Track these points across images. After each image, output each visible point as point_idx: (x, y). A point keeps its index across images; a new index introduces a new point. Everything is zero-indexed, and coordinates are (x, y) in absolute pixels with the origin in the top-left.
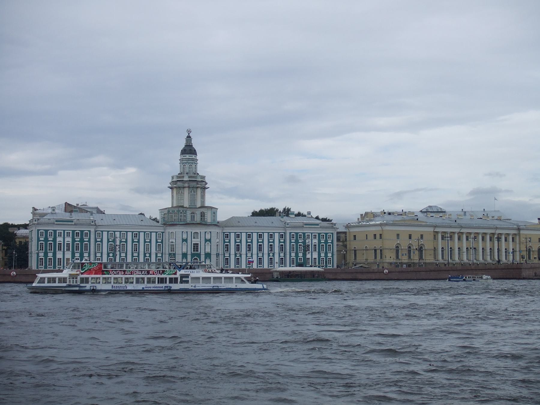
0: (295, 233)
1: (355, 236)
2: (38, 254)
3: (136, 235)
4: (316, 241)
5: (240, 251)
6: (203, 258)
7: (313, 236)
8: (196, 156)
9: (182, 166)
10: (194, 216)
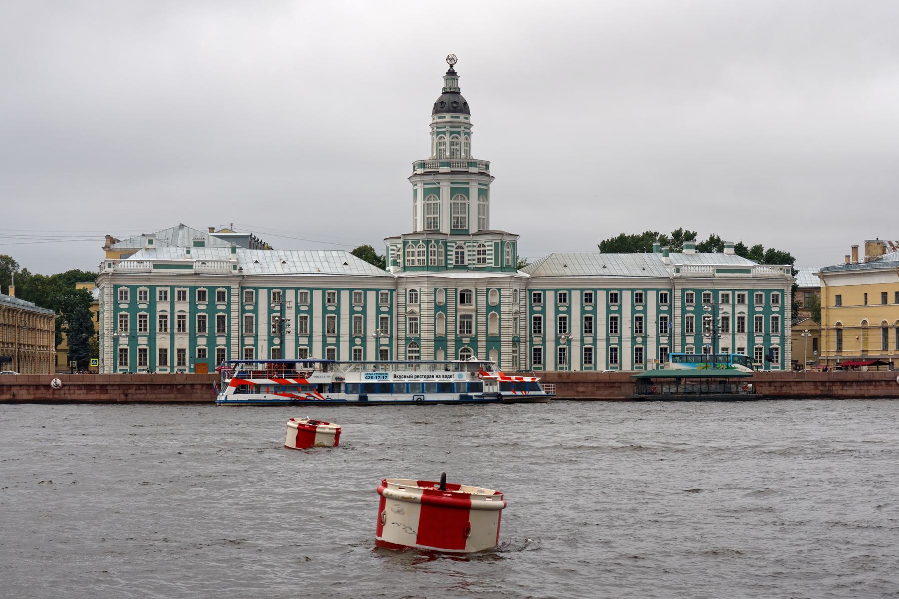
0: (694, 290)
1: (839, 298)
2: (116, 340)
3: (331, 297)
4: (742, 309)
5: (567, 332)
6: (482, 346)
8: (466, 116)
9: (436, 140)
10: (463, 253)
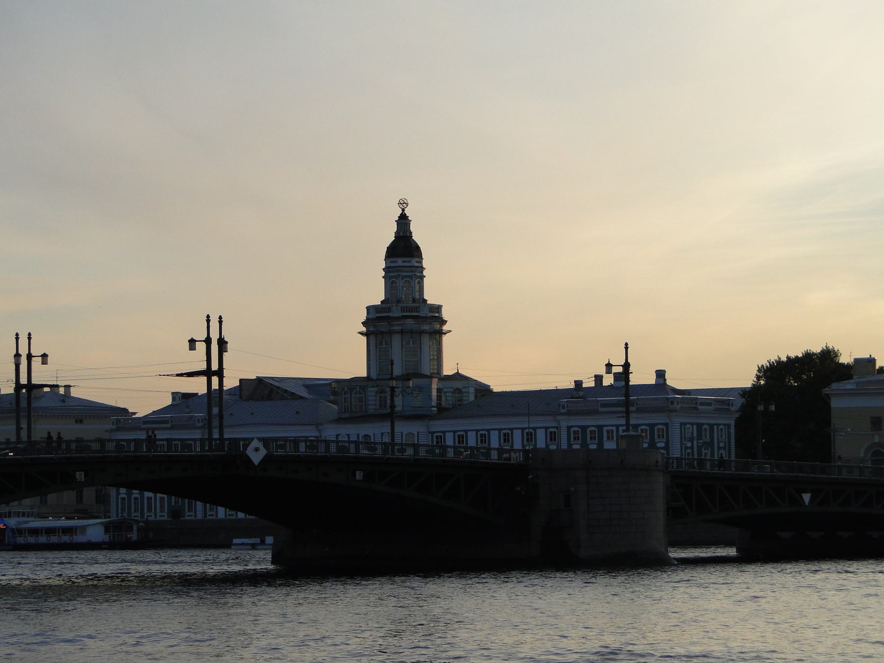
7: (572, 434)
